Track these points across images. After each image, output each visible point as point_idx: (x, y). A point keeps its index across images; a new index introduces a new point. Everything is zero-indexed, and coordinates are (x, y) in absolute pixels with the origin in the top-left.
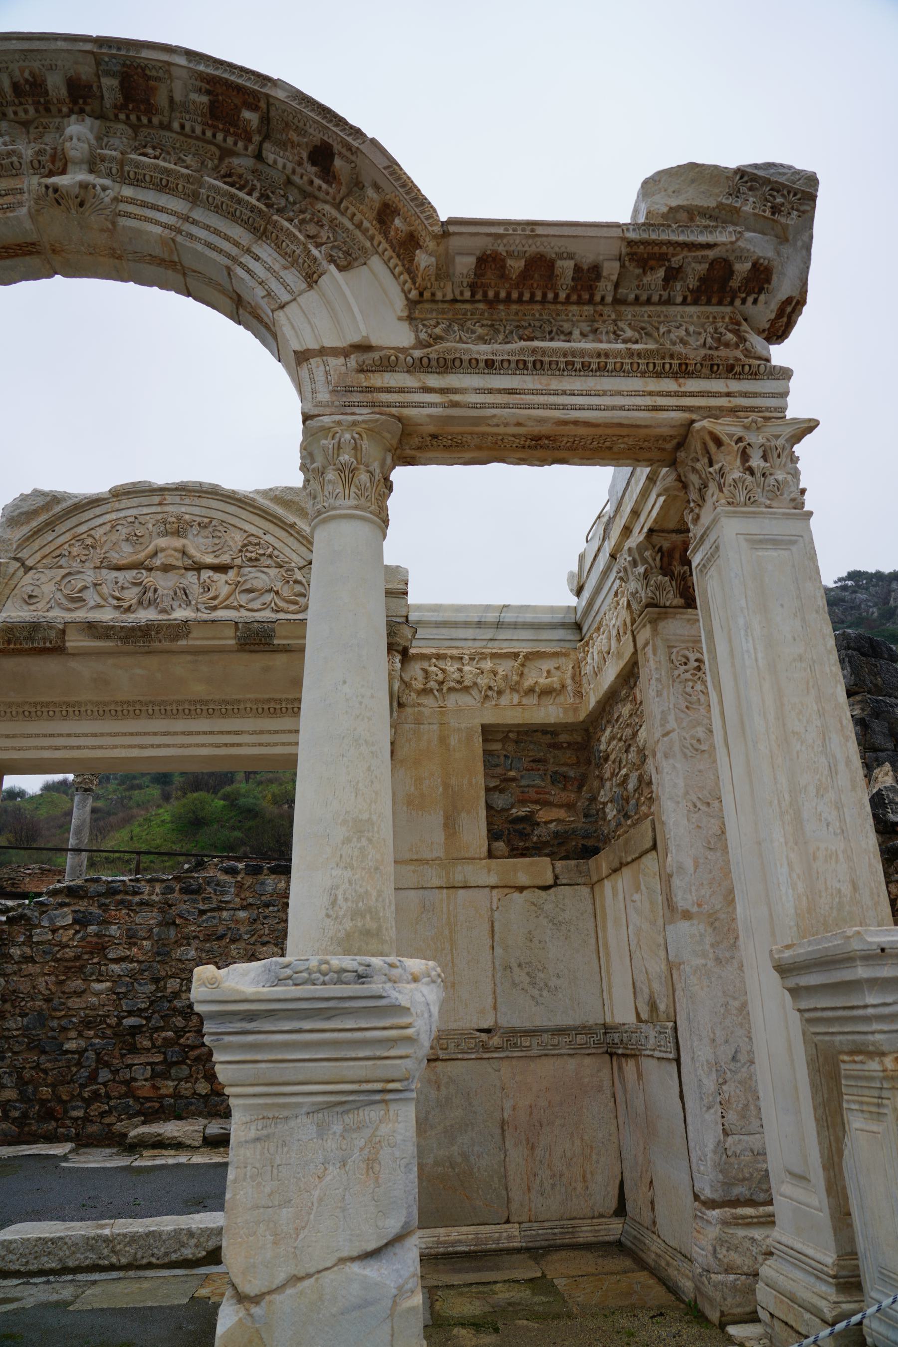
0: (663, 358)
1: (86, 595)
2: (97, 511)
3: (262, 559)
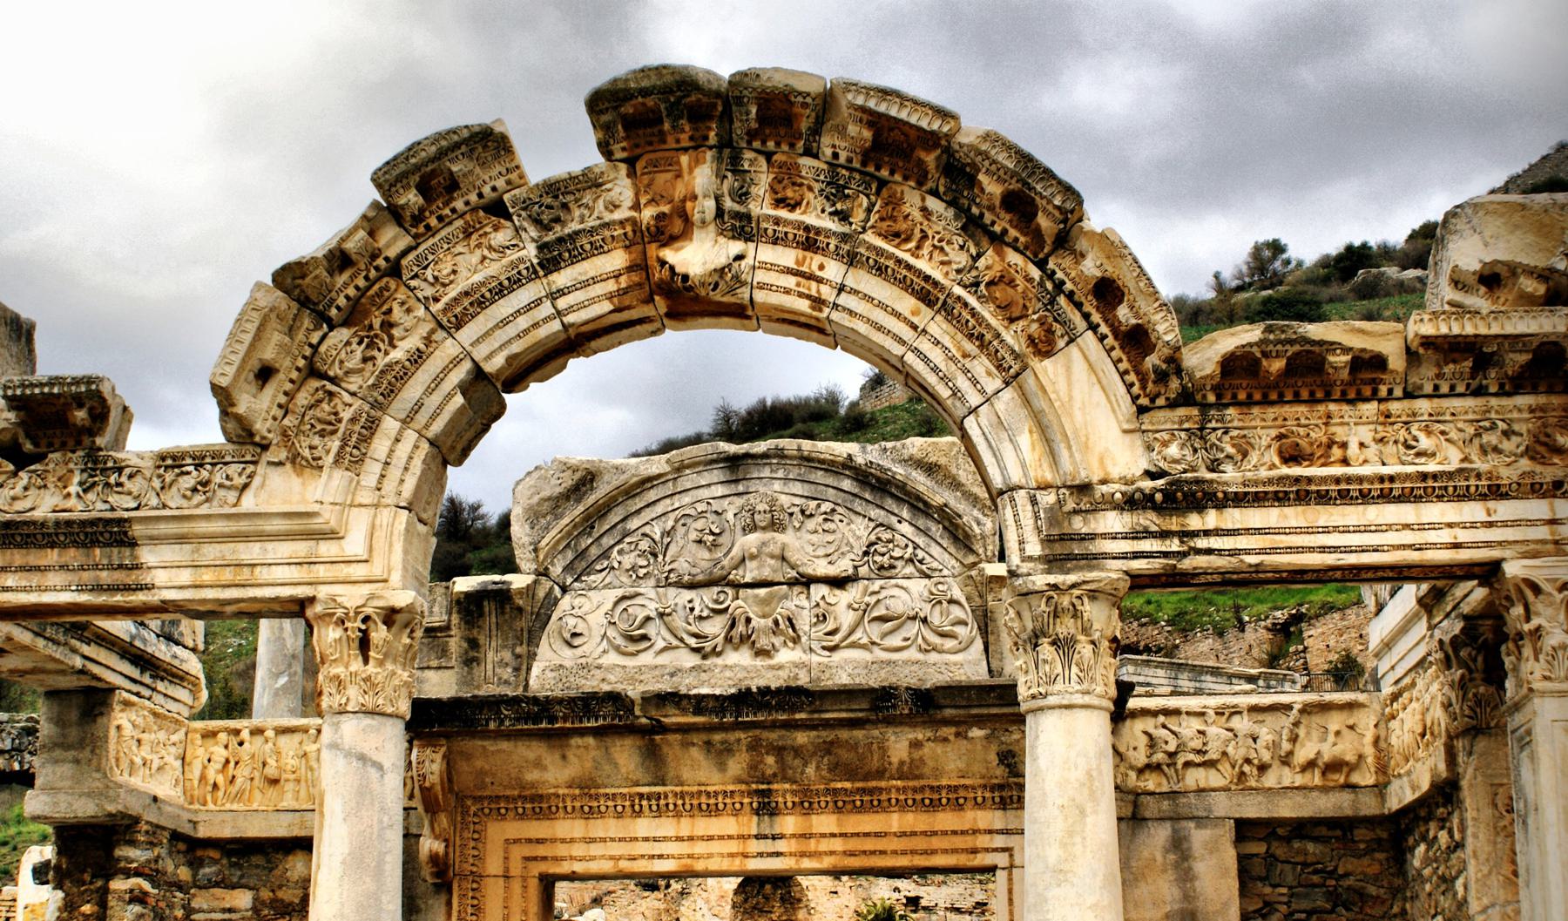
1: (651, 630)
2: (652, 495)
3: (899, 564)
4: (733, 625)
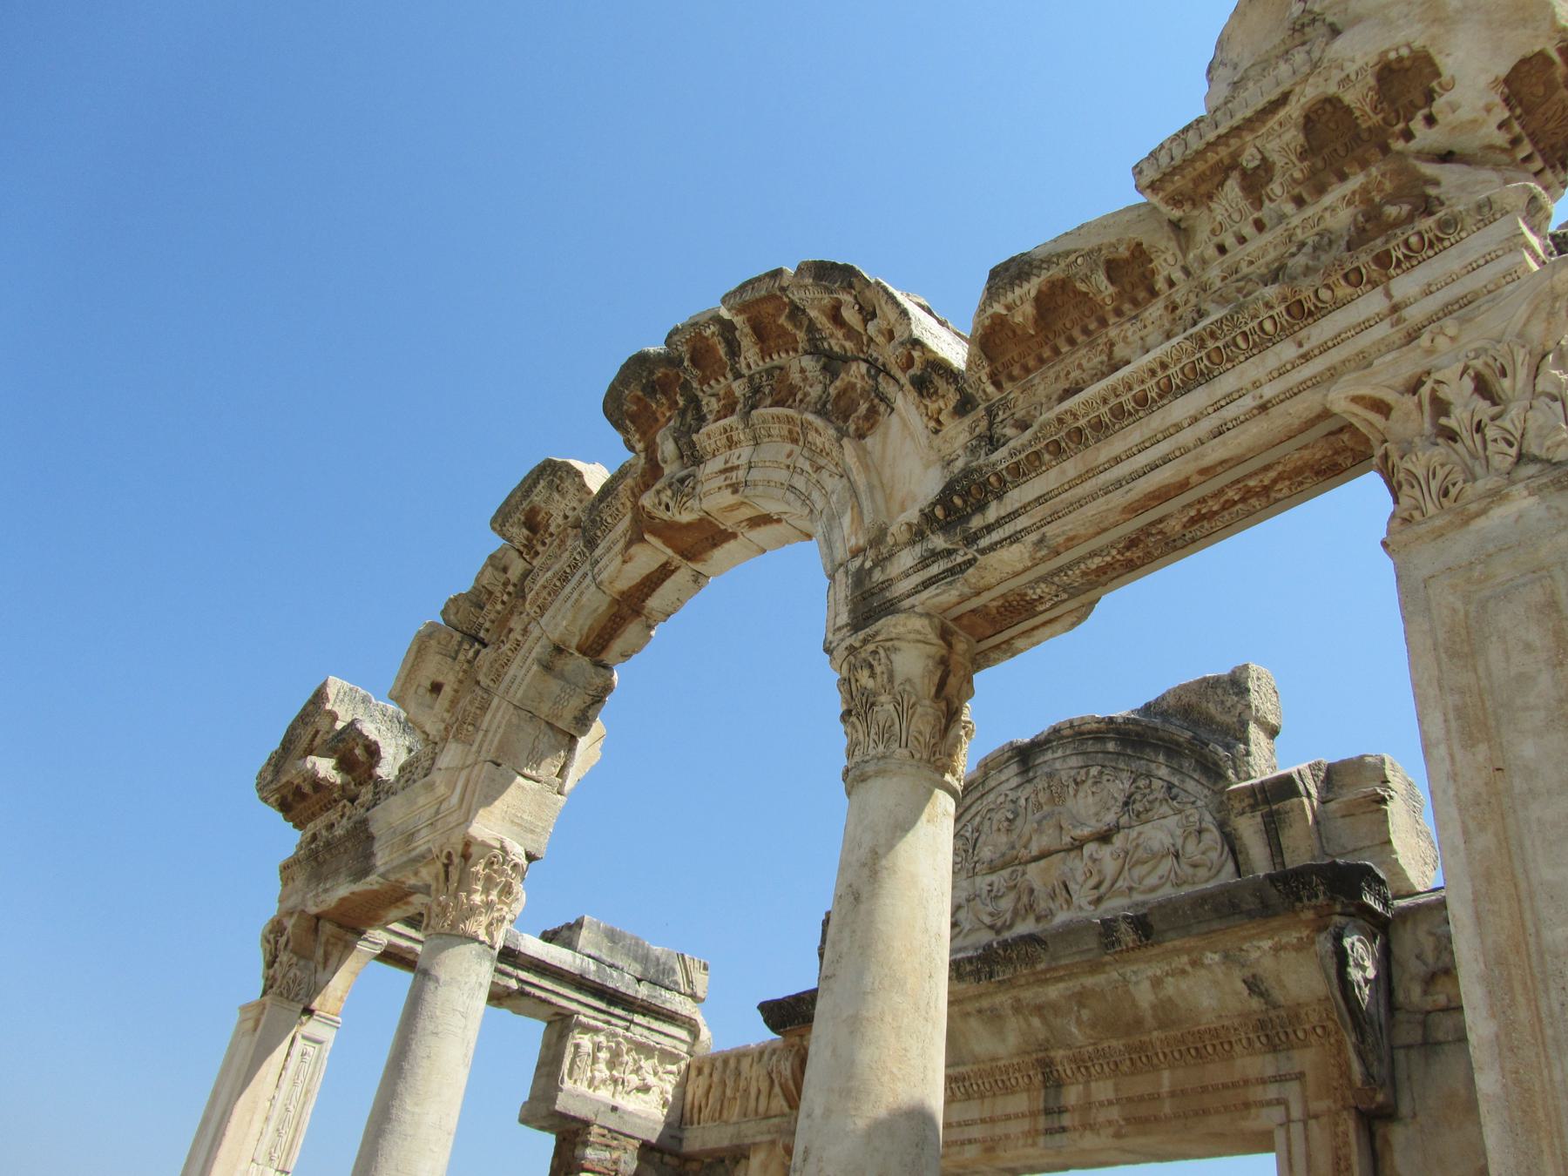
0: (1253, 317)
4: (1019, 899)
